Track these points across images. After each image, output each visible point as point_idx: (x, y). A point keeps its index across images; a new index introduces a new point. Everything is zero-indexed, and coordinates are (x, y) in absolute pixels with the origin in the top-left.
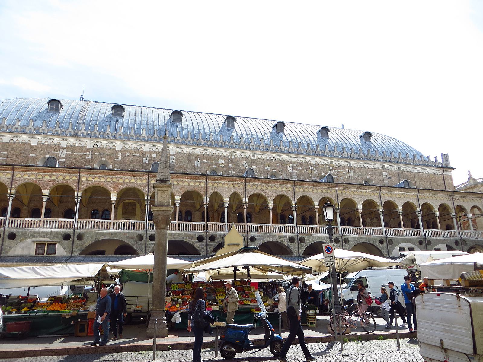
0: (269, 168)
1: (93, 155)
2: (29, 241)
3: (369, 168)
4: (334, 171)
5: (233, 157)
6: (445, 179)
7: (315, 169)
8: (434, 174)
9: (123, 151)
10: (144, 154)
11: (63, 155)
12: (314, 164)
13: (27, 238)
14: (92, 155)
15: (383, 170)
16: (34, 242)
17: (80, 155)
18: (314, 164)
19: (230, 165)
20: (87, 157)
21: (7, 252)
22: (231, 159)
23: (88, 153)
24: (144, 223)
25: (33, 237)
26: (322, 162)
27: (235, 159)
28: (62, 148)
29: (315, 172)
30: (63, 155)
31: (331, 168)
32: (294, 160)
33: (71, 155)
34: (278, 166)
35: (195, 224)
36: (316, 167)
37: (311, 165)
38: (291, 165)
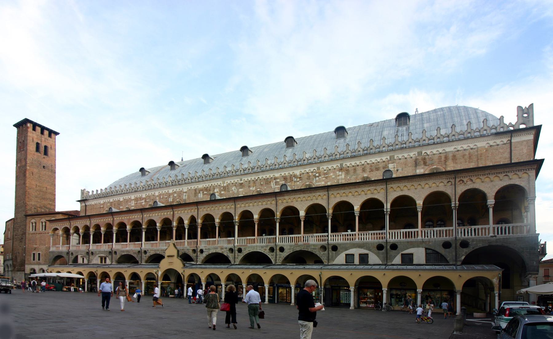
0: (254, 189)
2: (98, 256)
3: (368, 164)
4: (320, 177)
5: (225, 185)
6: (513, 149)
7: (298, 180)
8: (491, 146)
9: (160, 195)
10: (169, 195)
11: (133, 205)
12: (298, 174)
15: (390, 162)
18: (298, 174)
19: (222, 192)
22: (224, 187)
24: (417, 232)
26: (307, 170)
27: (227, 186)
29: (298, 183)
30: (133, 205)
31: (317, 175)
32: (277, 175)
34: (262, 185)
35: (406, 232)
36: (300, 178)
37: (295, 176)
38: (274, 181)
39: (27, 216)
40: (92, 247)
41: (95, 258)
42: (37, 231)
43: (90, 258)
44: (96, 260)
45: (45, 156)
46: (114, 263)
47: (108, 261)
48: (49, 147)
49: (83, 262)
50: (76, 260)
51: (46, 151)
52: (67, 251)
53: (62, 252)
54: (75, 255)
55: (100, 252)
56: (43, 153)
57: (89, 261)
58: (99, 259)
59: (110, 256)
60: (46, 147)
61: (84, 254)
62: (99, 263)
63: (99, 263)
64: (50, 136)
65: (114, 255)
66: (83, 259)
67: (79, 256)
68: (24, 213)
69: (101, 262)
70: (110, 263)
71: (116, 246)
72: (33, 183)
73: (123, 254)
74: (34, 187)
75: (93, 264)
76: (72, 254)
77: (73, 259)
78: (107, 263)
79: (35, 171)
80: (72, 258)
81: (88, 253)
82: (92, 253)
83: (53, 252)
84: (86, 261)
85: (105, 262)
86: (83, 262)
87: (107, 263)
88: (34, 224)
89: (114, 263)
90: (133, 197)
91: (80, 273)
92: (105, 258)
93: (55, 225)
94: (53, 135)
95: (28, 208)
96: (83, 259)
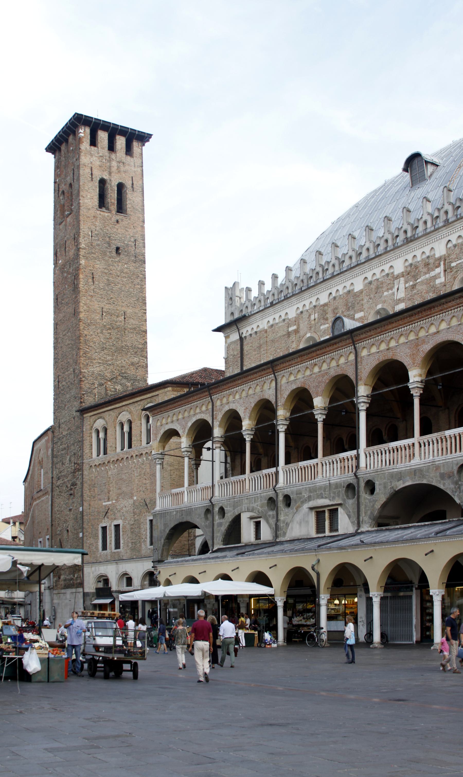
1: (449, 271)
2: (306, 506)
13: (303, 503)
14: (445, 271)
16: (311, 509)
17: (427, 279)
20: (438, 281)
21: (285, 534)
23: (437, 270)
25: (309, 499)
28: (398, 277)
33: (413, 287)
39: (83, 411)
40: (286, 476)
41: (298, 517)
42: (111, 456)
43: (282, 518)
44: (301, 524)
45: (120, 217)
46: (365, 528)
47: (345, 524)
48: (128, 184)
49: (258, 535)
50: (233, 533)
51: (118, 199)
52: (206, 503)
53: (190, 511)
54: (229, 517)
55: (316, 492)
56: (114, 208)
57: (276, 530)
58: (312, 519)
59: (351, 502)
60: (120, 187)
61: (260, 505)
62: (313, 534)
63: (313, 534)
64: (129, 150)
65: (365, 496)
66: (258, 525)
67: (244, 518)
68: (76, 405)
69: (320, 528)
70: (351, 529)
71: (369, 459)
72: (96, 306)
73: (400, 485)
74: (98, 317)
75: (291, 541)
76: (222, 511)
77: (223, 528)
78: (341, 531)
79: (99, 266)
80: (222, 525)
81: (272, 501)
82: (288, 500)
83: (163, 514)
84: (266, 533)
85: (334, 528)
86: (258, 535)
87: (341, 531)
88: (102, 435)
89: (365, 528)
90: (399, 266)
91: (260, 578)
92: (334, 512)
93: (162, 423)
94: (135, 144)
95: (85, 385)
96: (258, 525)
